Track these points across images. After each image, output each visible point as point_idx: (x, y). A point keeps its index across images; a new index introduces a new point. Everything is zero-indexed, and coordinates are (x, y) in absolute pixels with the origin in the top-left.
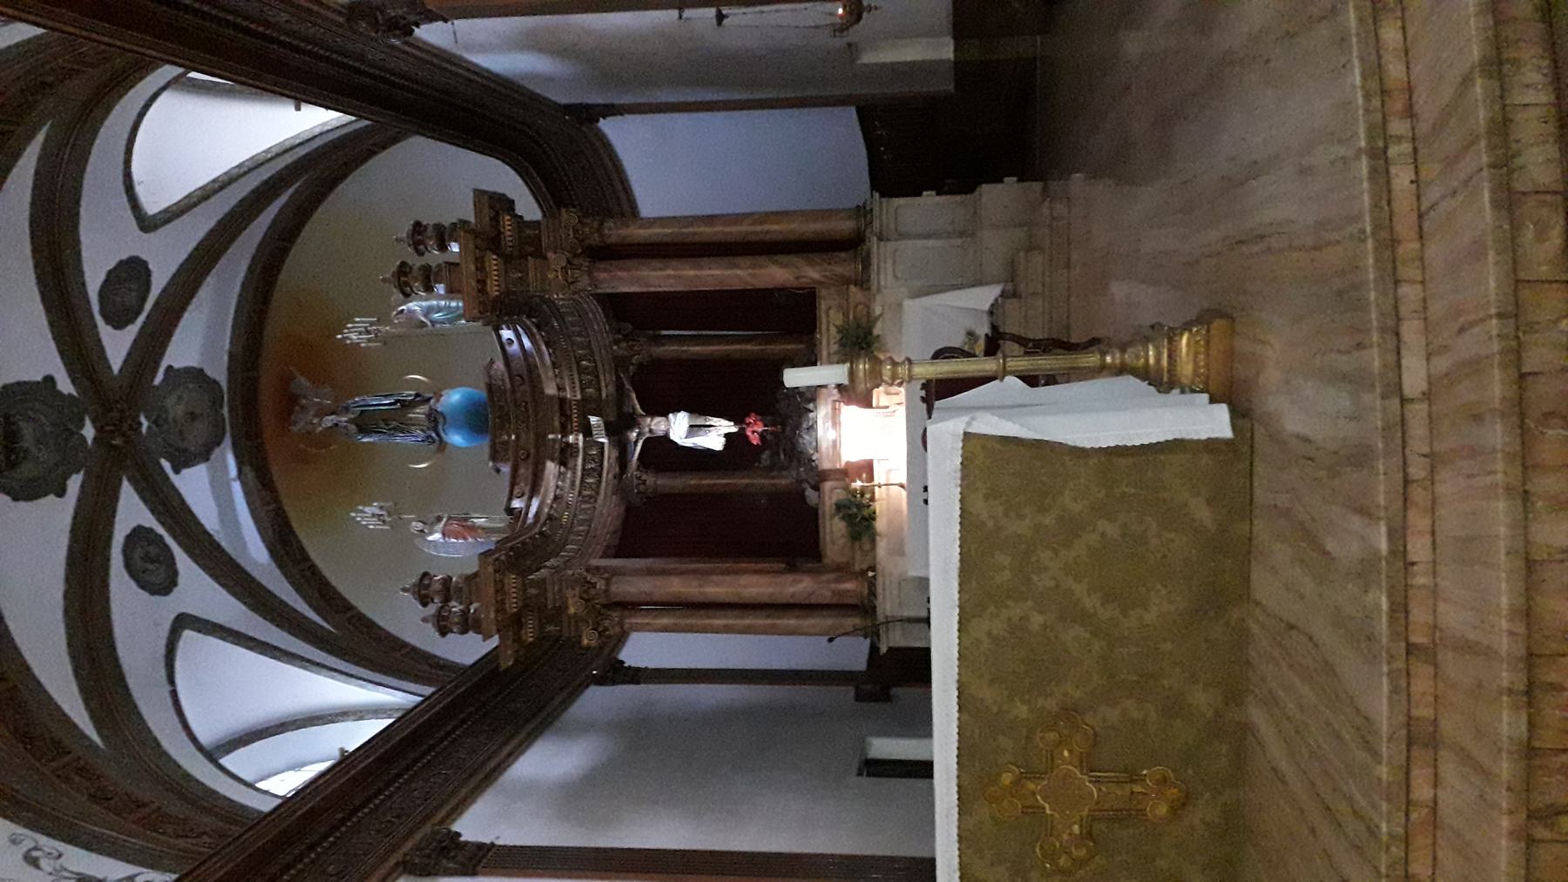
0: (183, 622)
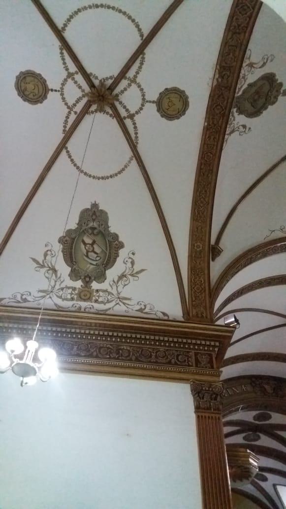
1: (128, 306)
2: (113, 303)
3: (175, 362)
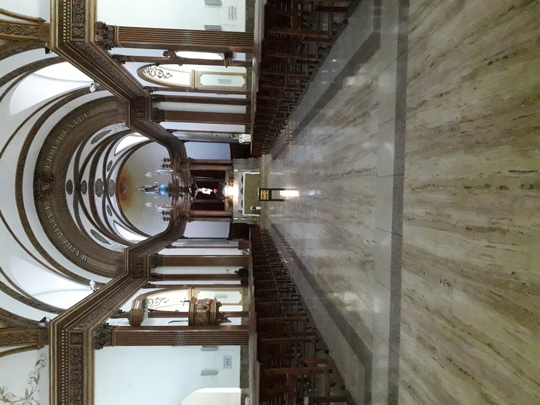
0: (114, 221)
1: (34, 390)
2: (32, 402)
3: (80, 358)
